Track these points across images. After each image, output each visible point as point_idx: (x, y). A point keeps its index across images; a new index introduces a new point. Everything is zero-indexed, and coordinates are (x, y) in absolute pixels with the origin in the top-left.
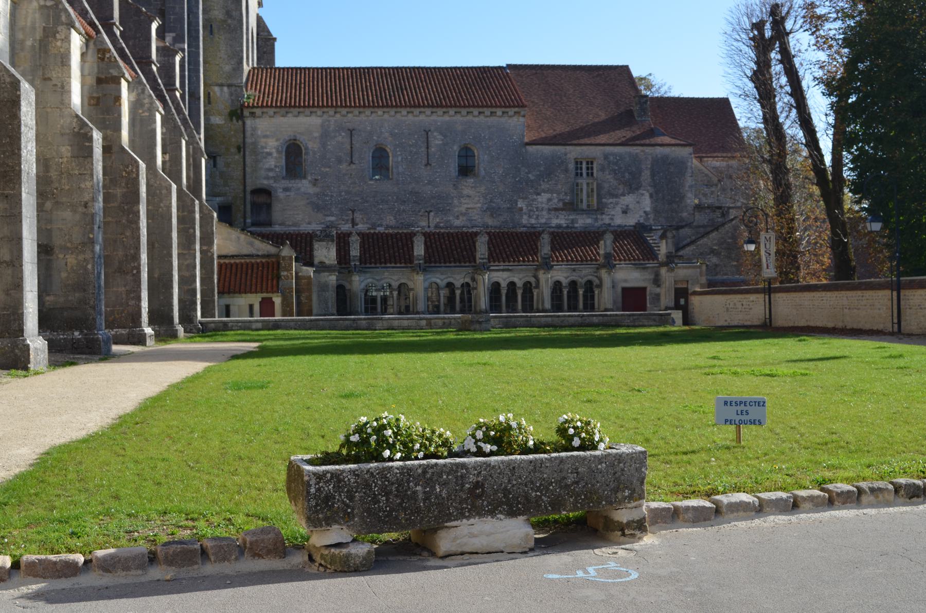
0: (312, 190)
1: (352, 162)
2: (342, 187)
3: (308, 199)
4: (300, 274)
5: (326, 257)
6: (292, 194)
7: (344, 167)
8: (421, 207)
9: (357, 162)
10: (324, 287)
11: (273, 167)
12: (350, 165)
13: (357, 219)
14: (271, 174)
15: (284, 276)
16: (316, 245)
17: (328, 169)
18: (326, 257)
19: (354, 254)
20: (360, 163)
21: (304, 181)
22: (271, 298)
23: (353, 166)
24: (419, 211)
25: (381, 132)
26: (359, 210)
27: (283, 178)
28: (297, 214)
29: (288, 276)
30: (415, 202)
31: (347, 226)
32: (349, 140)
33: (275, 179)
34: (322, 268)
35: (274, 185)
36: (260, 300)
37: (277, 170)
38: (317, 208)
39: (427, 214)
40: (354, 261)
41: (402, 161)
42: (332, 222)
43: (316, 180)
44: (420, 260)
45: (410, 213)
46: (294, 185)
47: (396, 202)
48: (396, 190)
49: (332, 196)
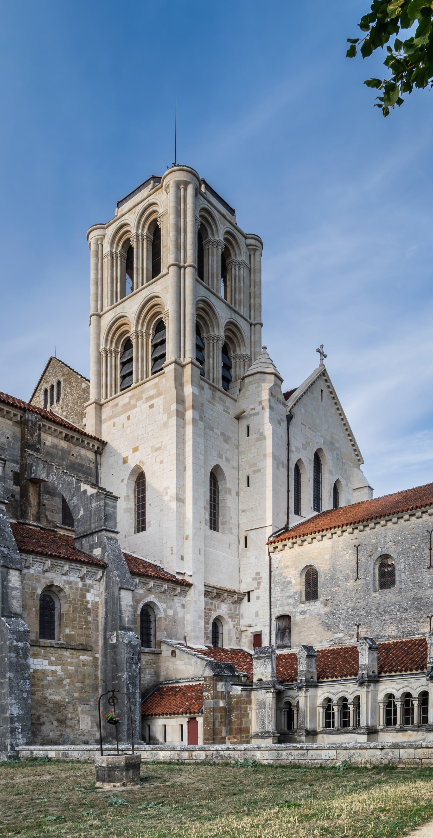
0: (324, 610)
1: (357, 577)
2: (350, 604)
3: (320, 619)
4: (231, 693)
5: (263, 674)
6: (307, 616)
7: (351, 584)
8: (422, 612)
9: (362, 577)
10: (262, 705)
11: (292, 594)
12: (356, 580)
13: (362, 633)
14: (291, 601)
15: (205, 696)
16: (255, 663)
17: (337, 589)
18: (263, 674)
19: (301, 669)
20: (365, 577)
21: (318, 603)
22: (195, 718)
23: (359, 581)
24: (421, 618)
25: (385, 542)
26: (364, 624)
27: (301, 603)
28: (311, 635)
29: (208, 696)
30: (417, 609)
31: (353, 640)
32: (356, 556)
33: (295, 606)
34: (262, 685)
35: (294, 610)
36: (187, 720)
37: (296, 596)
38: (328, 627)
39: (428, 619)
40: (300, 676)
41: (405, 568)
42: (340, 639)
43: (327, 600)
44: (364, 670)
45: (412, 620)
46: (310, 608)
47: (398, 611)
48: (398, 599)
49: (340, 614)
